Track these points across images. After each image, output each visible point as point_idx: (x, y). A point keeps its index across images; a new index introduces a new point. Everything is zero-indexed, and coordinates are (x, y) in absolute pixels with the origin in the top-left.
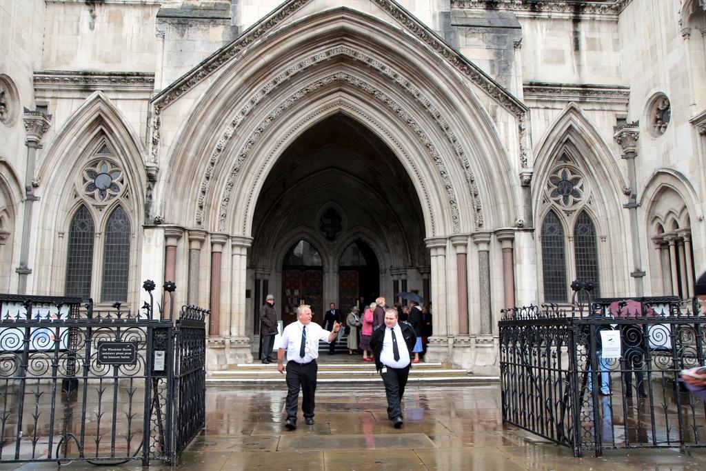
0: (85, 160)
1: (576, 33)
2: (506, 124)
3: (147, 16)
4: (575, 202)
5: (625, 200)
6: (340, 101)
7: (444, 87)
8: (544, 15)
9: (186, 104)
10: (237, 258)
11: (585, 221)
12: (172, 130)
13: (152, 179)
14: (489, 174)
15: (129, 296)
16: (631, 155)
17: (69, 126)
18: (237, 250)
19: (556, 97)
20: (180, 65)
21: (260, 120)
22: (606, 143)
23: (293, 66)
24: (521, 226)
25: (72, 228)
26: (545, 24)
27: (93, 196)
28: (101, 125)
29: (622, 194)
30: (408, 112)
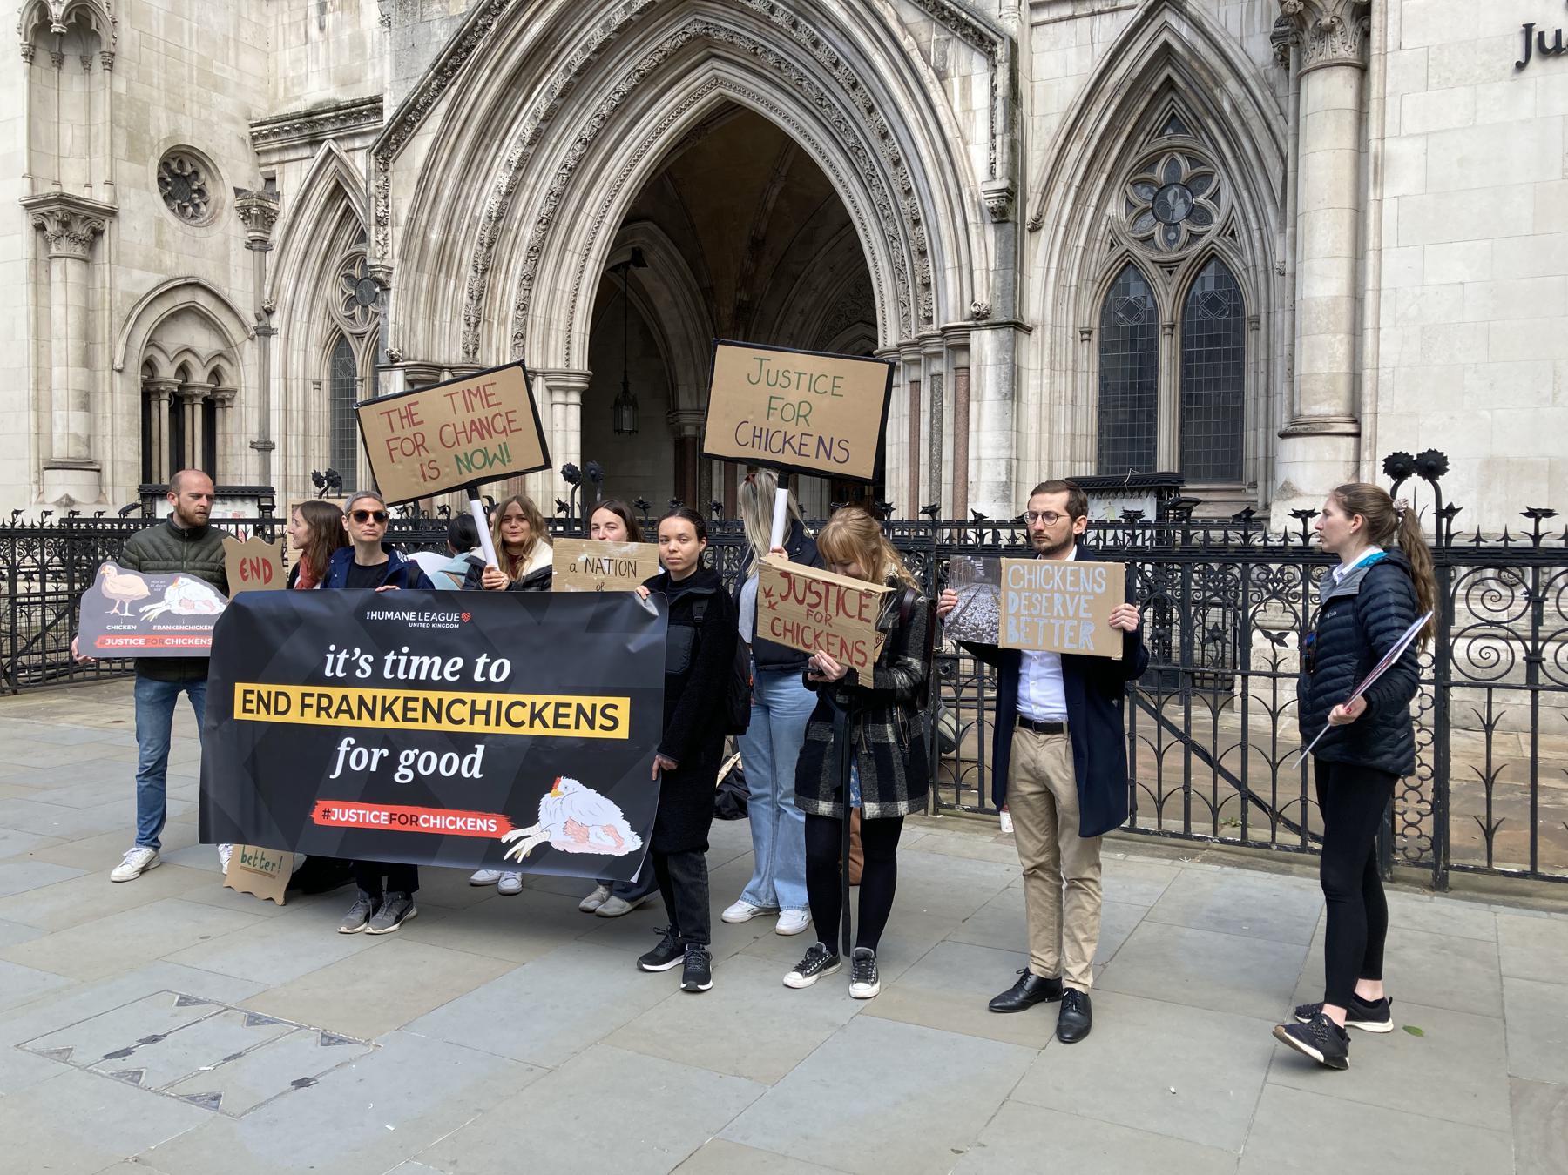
0: (337, 259)
2: (966, 80)
4: (1194, 237)
6: (717, 78)
9: (420, 147)
18: (559, 397)
21: (563, 149)
22: (1246, 75)
24: (978, 316)
27: (352, 317)
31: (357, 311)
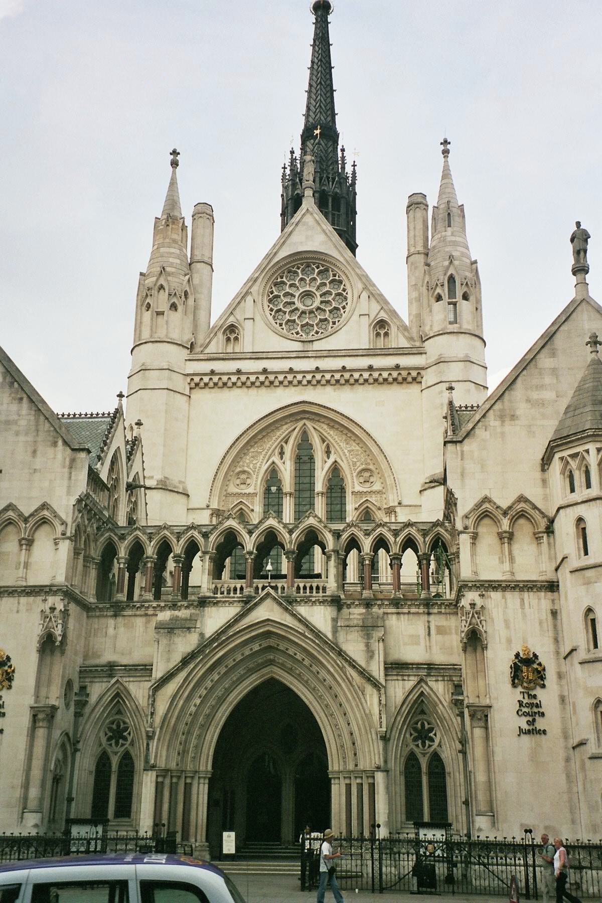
1: (429, 622)
2: (371, 695)
3: (148, 622)
4: (430, 746)
5: (460, 747)
7: (332, 670)
8: (406, 610)
9: (171, 688)
10: (201, 786)
11: (436, 760)
12: (162, 707)
13: (150, 737)
14: (359, 729)
15: (132, 814)
16: (461, 715)
17: (101, 699)
18: (202, 781)
19: (410, 672)
20: (168, 660)
21: (219, 692)
23: (239, 657)
25: (97, 767)
26: (406, 616)
27: (111, 745)
28: (119, 699)
29: (457, 742)
30: (313, 682)
31: (113, 742)
